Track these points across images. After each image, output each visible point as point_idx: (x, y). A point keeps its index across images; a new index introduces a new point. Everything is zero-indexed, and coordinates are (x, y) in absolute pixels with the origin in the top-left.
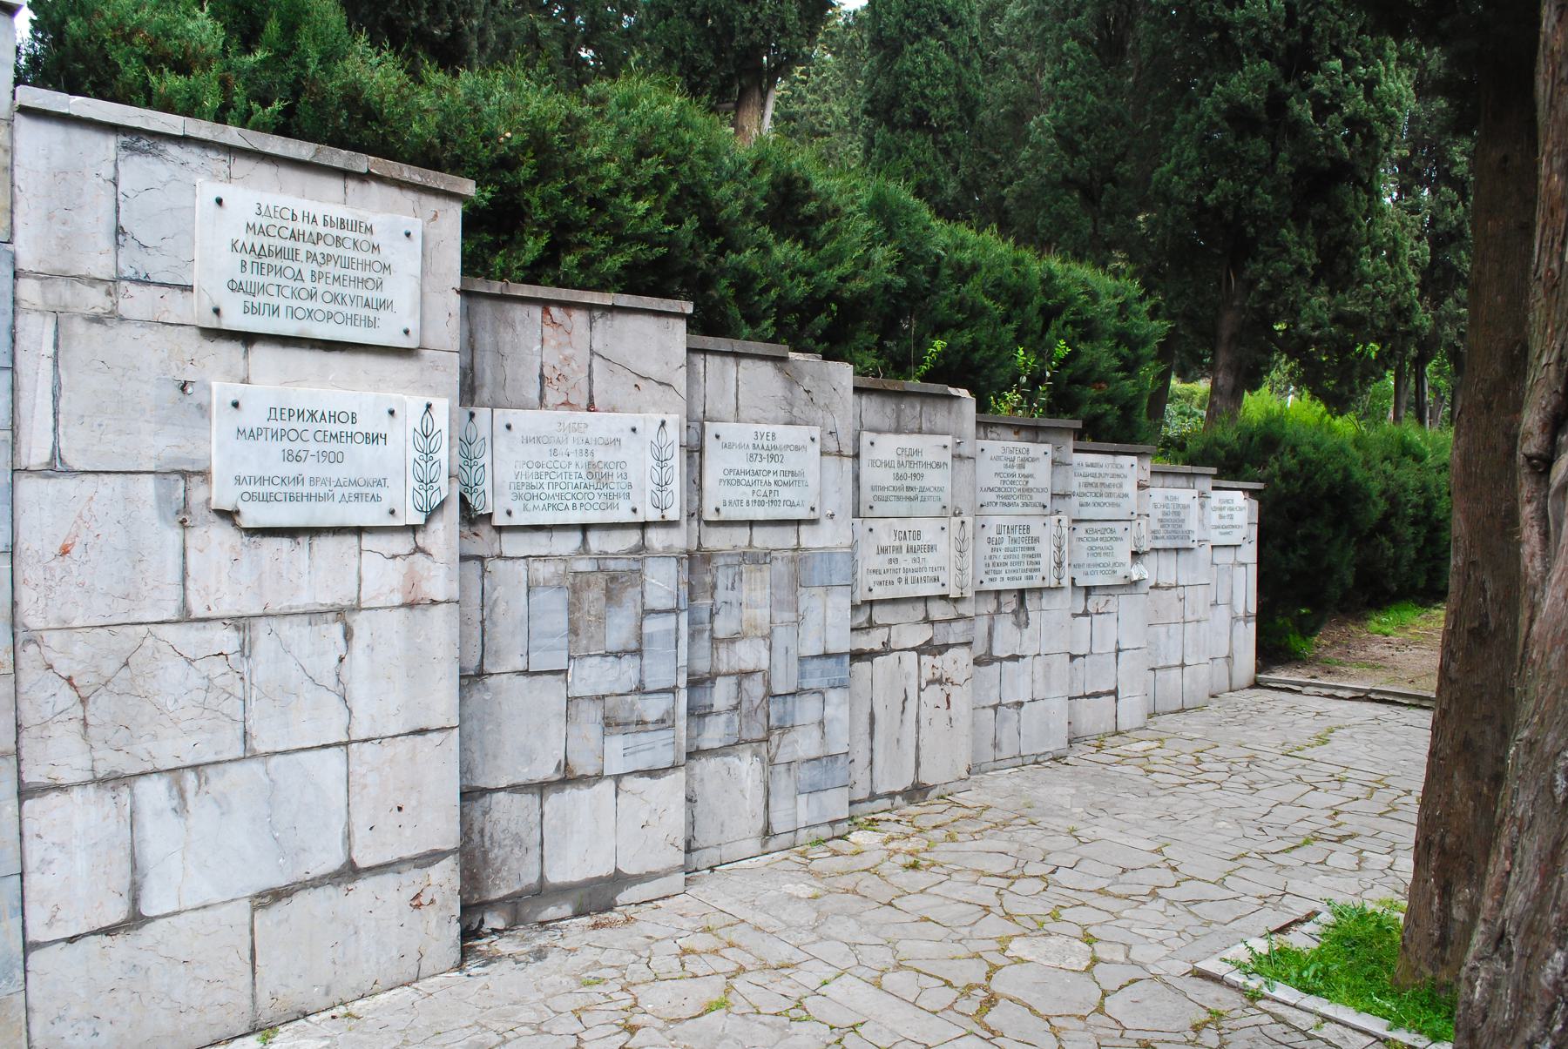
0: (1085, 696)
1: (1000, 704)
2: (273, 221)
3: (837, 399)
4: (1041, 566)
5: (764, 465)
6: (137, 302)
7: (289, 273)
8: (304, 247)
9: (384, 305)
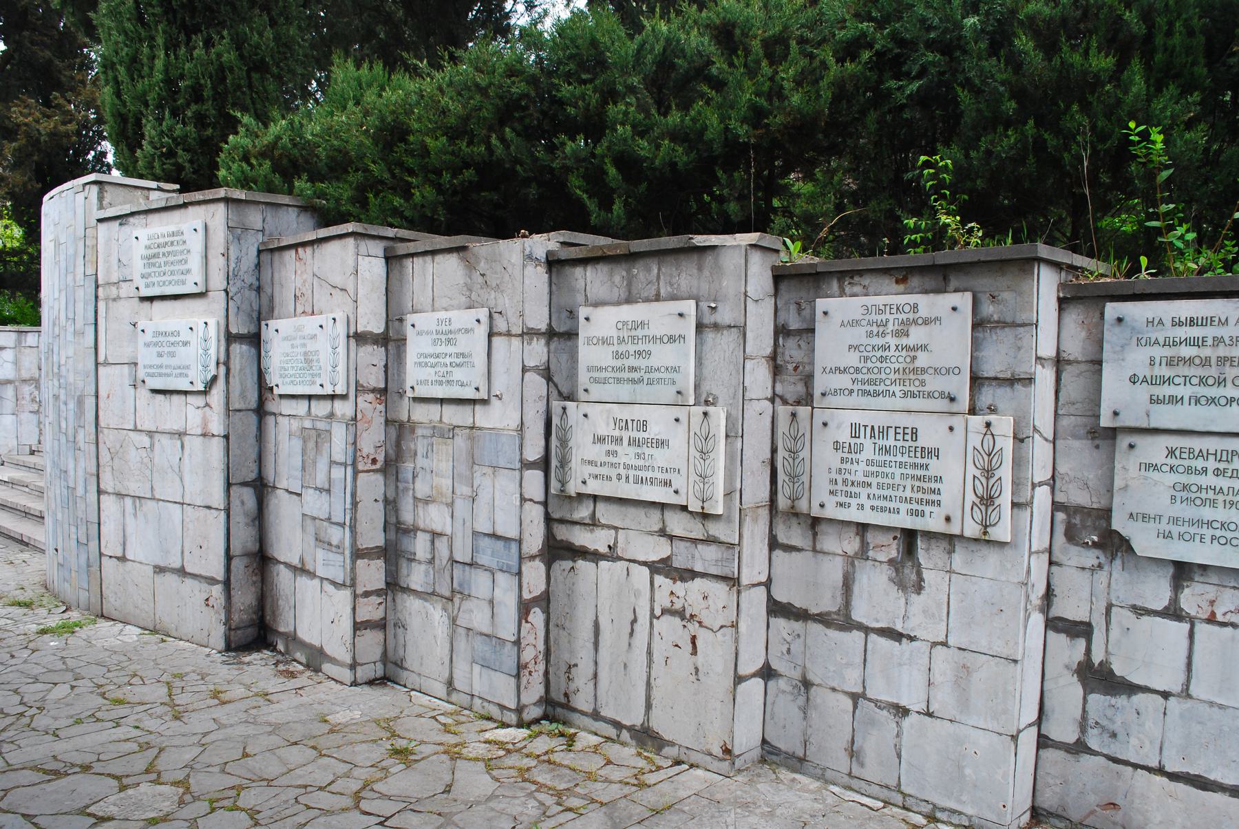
0: (1160, 771)
3: (507, 277)
4: (943, 498)
5: (442, 349)
9: (188, 271)
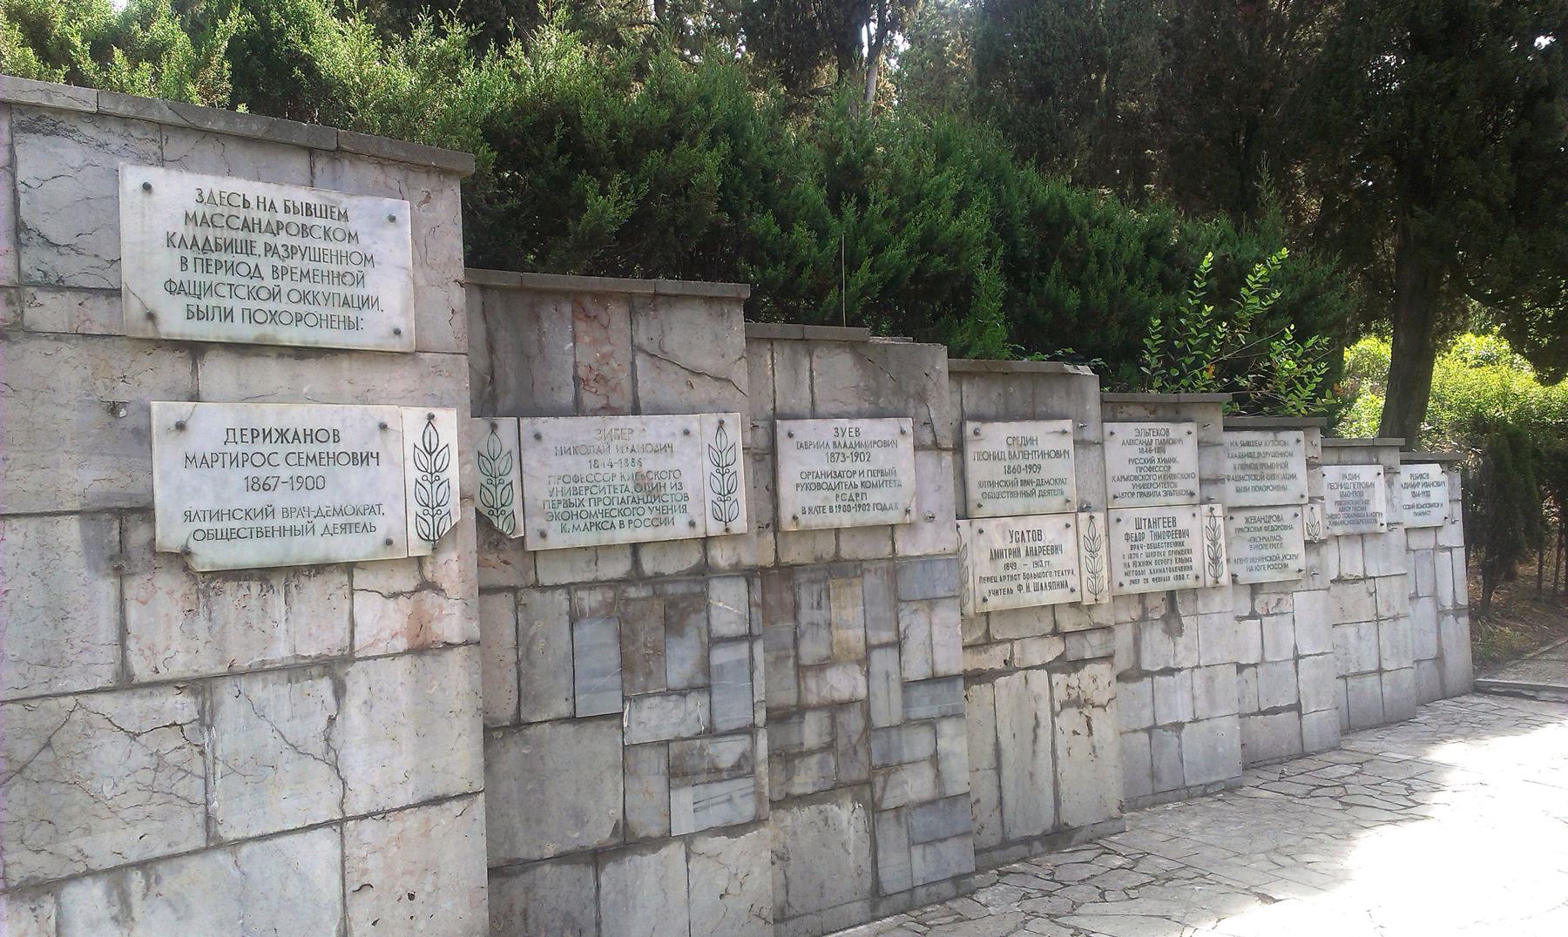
1: (1155, 726)
2: (219, 210)
5: (848, 465)
6: (50, 311)
7: (243, 269)
8: (260, 240)
9: (366, 302)
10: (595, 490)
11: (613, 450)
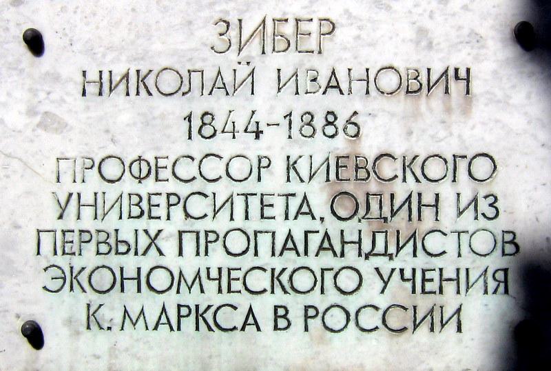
10: (198, 206)
11: (266, 81)
